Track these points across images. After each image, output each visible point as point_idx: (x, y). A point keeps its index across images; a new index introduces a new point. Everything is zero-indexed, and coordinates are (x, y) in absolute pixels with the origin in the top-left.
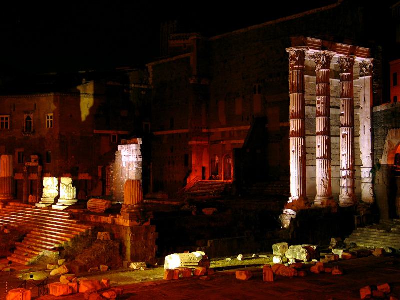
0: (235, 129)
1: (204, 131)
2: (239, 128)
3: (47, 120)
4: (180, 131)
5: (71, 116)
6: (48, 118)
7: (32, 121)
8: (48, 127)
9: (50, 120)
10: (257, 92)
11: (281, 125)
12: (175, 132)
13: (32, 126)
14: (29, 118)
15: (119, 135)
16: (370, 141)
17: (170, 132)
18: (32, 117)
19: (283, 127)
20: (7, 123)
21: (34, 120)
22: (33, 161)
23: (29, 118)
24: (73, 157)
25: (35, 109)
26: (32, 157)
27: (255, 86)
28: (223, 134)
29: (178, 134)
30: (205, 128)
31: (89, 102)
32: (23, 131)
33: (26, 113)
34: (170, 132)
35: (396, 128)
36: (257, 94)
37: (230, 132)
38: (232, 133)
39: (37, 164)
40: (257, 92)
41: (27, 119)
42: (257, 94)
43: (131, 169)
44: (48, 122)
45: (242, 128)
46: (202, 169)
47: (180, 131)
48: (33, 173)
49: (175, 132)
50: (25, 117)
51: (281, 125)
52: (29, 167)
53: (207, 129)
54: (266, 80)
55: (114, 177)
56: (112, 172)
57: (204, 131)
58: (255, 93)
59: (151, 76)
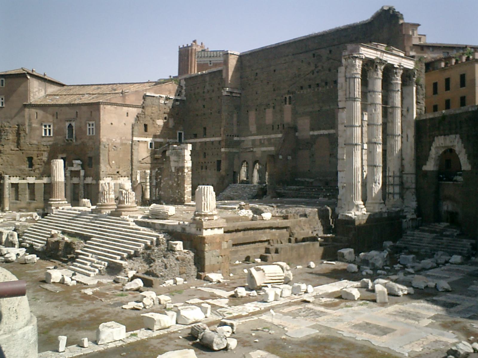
0: (265, 138)
1: (236, 139)
2: (269, 136)
3: (88, 127)
5: (112, 124)
6: (89, 126)
7: (74, 128)
8: (90, 133)
9: (91, 127)
10: (288, 103)
11: (311, 133)
12: (208, 140)
13: (74, 133)
14: (70, 126)
15: (155, 142)
16: (413, 149)
17: (203, 140)
18: (73, 124)
20: (50, 130)
21: (75, 127)
22: (75, 165)
23: (70, 126)
24: (113, 162)
25: (77, 117)
26: (74, 162)
27: (286, 97)
28: (254, 141)
30: (236, 136)
31: (128, 110)
32: (65, 137)
33: (68, 121)
34: (203, 140)
35: (445, 135)
36: (288, 105)
37: (260, 140)
38: (263, 142)
39: (79, 168)
41: (68, 127)
42: (288, 105)
43: (180, 174)
44: (89, 129)
45: (273, 136)
46: (233, 173)
48: (75, 177)
49: (208, 140)
50: (67, 124)
51: (311, 133)
52: (71, 171)
53: (238, 136)
54: (297, 92)
55: (162, 181)
56: (160, 176)
57: (236, 139)
58: (286, 104)
59: (184, 88)
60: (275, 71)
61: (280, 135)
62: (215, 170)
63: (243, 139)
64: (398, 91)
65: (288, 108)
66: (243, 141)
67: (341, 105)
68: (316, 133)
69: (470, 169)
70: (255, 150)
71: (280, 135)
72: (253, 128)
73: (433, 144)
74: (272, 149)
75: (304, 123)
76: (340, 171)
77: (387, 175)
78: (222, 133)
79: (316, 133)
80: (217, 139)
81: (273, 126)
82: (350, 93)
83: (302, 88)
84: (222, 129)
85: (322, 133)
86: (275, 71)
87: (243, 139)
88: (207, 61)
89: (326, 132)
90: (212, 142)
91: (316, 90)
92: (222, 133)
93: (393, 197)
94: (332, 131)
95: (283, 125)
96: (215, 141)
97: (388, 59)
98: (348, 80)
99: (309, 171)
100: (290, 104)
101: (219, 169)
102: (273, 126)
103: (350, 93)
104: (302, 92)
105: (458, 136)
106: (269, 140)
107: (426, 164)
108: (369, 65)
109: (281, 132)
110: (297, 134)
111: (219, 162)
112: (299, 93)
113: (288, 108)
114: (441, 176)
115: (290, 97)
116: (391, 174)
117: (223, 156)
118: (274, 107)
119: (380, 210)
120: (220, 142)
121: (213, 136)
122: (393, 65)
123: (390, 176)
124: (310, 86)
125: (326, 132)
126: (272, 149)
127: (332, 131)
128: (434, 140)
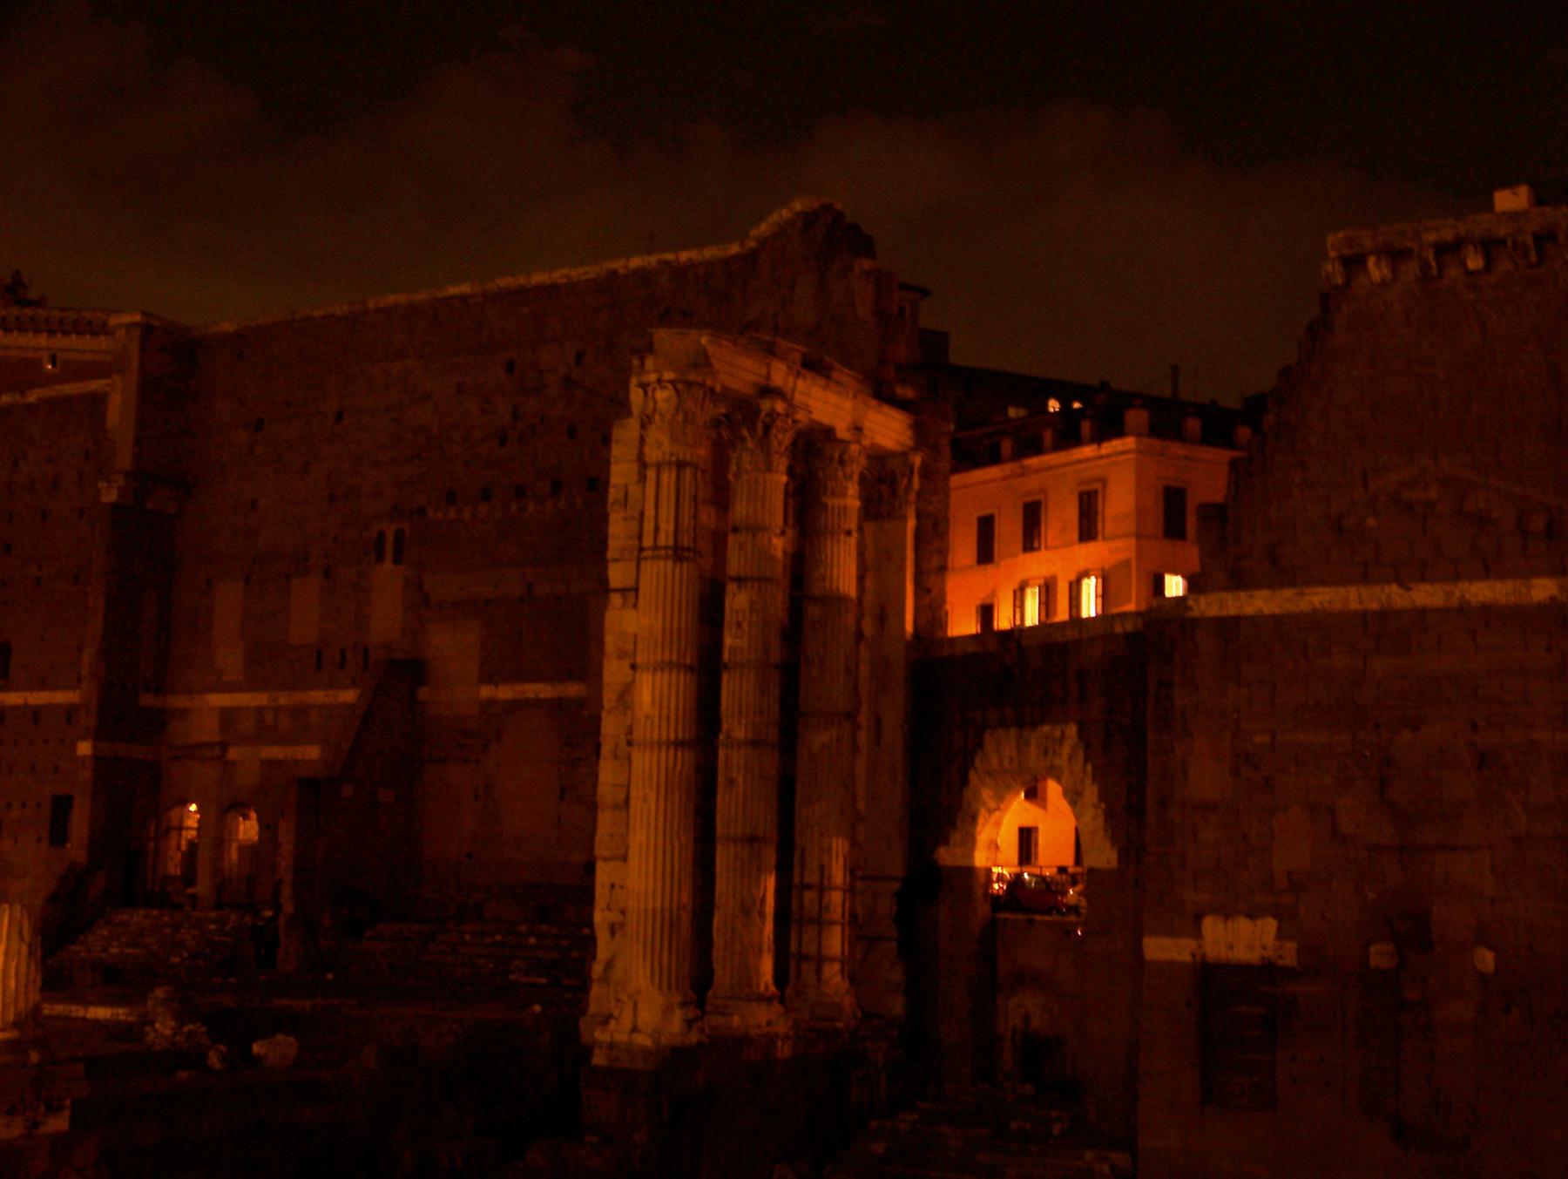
0: (282, 701)
1: (147, 700)
2: (300, 697)
4: (39, 698)
10: (389, 555)
11: (486, 692)
19: (493, 701)
27: (382, 534)
28: (228, 716)
29: (26, 706)
35: (1021, 725)
36: (388, 565)
37: (260, 710)
38: (269, 718)
40: (389, 555)
42: (388, 565)
45: (317, 696)
47: (39, 698)
51: (486, 692)
57: (147, 700)
58: (380, 559)
60: (339, 417)
61: (349, 696)
62: (39, 840)
63: (178, 702)
64: (849, 533)
65: (388, 579)
66: (182, 714)
67: (617, 575)
68: (505, 693)
69: (1114, 864)
70: (233, 753)
71: (349, 696)
72: (230, 659)
73: (977, 763)
74: (313, 752)
75: (454, 648)
76: (605, 860)
77: (796, 880)
78: (85, 671)
79: (505, 693)
80: (63, 697)
81: (319, 653)
82: (657, 529)
83: (452, 498)
84: (88, 656)
85: (531, 695)
86: (339, 417)
87: (178, 702)
88: (36, 349)
89: (544, 691)
90: (36, 714)
91: (514, 507)
92: (85, 671)
93: (819, 972)
94: (573, 690)
95: (366, 653)
96: (48, 706)
97: (811, 402)
98: (651, 473)
99: (469, 856)
100: (397, 559)
101: (58, 835)
102: (319, 653)
103: (657, 529)
104: (452, 514)
105: (1072, 730)
106: (300, 711)
107: (947, 842)
108: (740, 418)
109: (354, 685)
110: (424, 693)
111: (61, 806)
112: (440, 515)
113: (388, 579)
114: (1012, 412)
115: (399, 537)
116: (812, 877)
117: (86, 775)
118: (327, 574)
119: (766, 1030)
120: (70, 712)
121: (43, 685)
122: (828, 432)
123: (809, 887)
124: (486, 495)
125: (544, 691)
126: (313, 752)
127: (573, 690)
128: (980, 745)
